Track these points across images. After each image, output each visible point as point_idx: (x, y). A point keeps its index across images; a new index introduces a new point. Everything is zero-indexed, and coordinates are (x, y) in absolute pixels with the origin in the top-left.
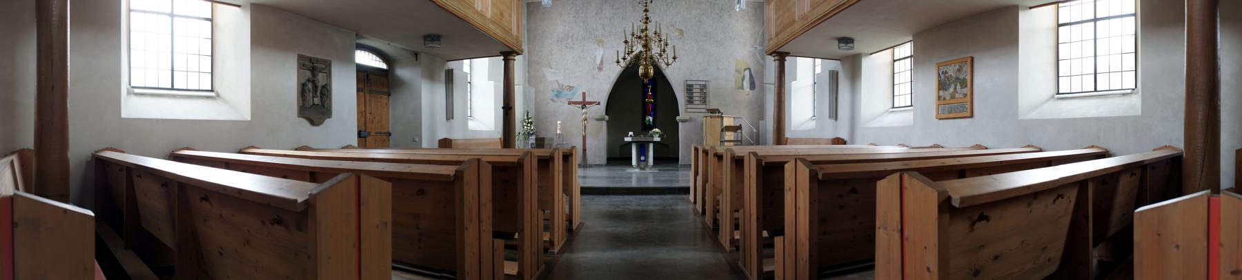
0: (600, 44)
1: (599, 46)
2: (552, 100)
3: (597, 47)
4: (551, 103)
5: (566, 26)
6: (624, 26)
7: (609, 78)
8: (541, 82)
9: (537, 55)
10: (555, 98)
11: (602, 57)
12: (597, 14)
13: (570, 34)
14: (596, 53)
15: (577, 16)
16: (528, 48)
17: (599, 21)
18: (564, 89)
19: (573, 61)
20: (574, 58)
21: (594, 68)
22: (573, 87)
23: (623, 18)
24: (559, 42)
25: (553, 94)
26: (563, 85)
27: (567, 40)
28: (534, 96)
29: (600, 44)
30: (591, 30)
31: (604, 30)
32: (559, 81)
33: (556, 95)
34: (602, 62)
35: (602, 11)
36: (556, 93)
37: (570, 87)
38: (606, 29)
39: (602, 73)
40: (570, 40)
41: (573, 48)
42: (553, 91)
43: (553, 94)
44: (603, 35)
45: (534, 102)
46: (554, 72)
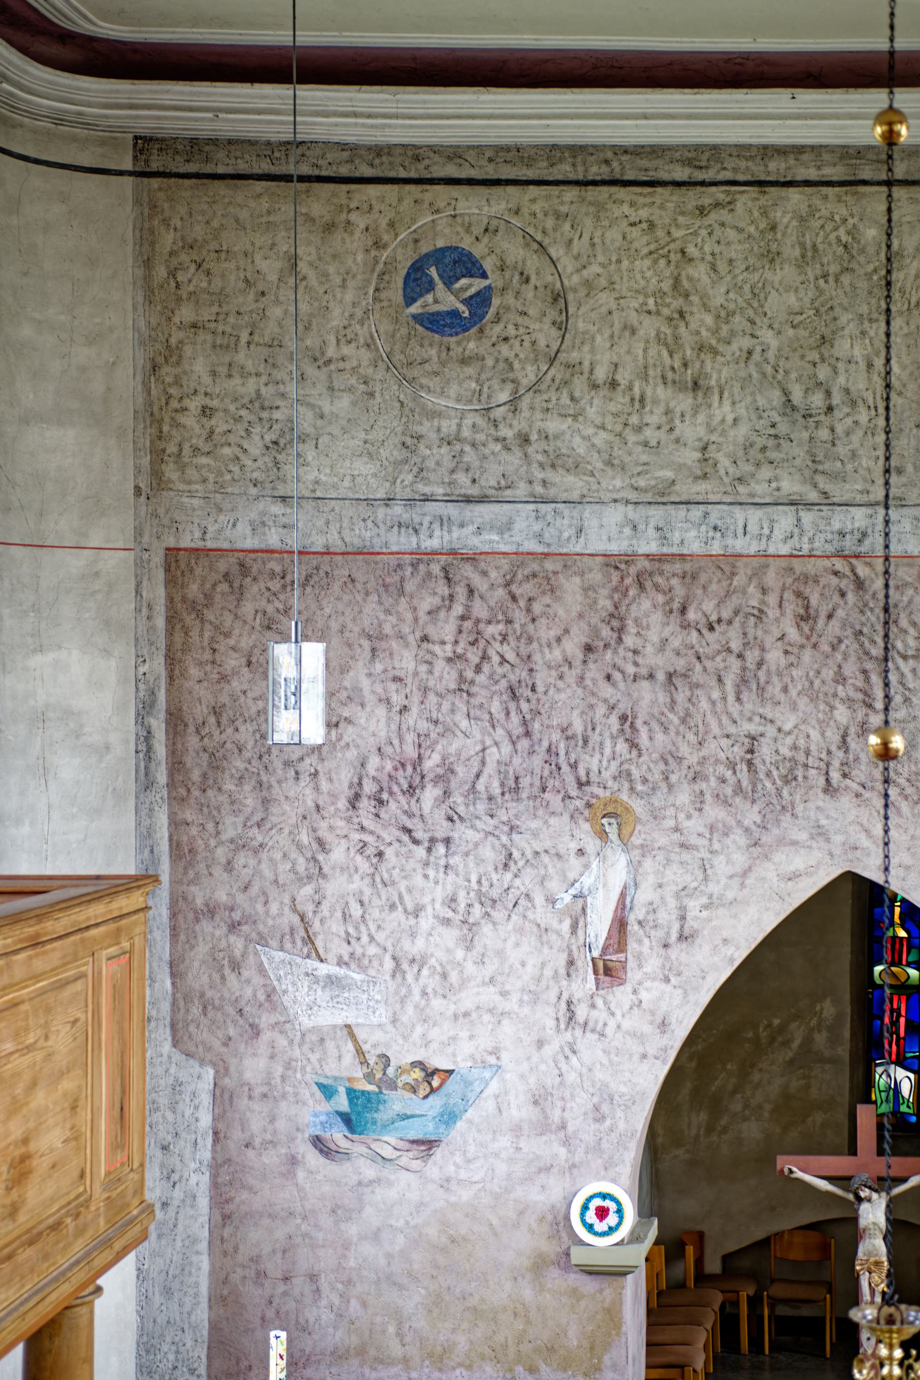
0: (612, 831)
1: (603, 835)
2: (318, 1142)
3: (591, 844)
4: (313, 1158)
5: (404, 709)
6: (752, 728)
7: (663, 1025)
8: (256, 1031)
9: (229, 866)
10: (338, 1136)
11: (623, 895)
12: (588, 649)
13: (431, 762)
14: (587, 881)
15: (475, 660)
16: (176, 824)
17: (607, 691)
18: (393, 1086)
19: (447, 922)
20: (452, 901)
21: (571, 963)
22: (450, 1072)
23: (744, 681)
24: (365, 804)
25: (324, 1107)
26: (385, 1060)
27: (411, 790)
28: (206, 1120)
29: (612, 831)
30: (556, 736)
31: (633, 745)
32: (361, 1035)
33: (346, 1119)
34: (620, 925)
35: (621, 630)
36: (342, 1103)
37: (430, 1074)
38: (643, 738)
39: (621, 996)
40: (430, 795)
41: (447, 841)
42: (327, 1091)
43: (324, 1107)
44: (624, 775)
45: (206, 1154)
46: (331, 981)
